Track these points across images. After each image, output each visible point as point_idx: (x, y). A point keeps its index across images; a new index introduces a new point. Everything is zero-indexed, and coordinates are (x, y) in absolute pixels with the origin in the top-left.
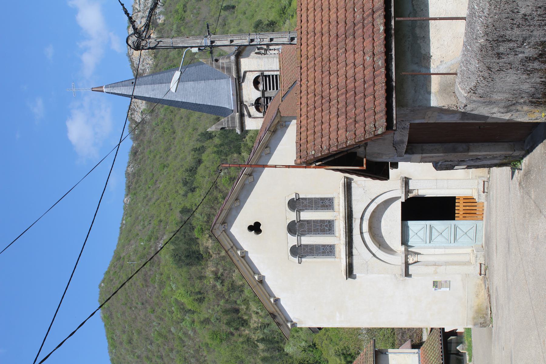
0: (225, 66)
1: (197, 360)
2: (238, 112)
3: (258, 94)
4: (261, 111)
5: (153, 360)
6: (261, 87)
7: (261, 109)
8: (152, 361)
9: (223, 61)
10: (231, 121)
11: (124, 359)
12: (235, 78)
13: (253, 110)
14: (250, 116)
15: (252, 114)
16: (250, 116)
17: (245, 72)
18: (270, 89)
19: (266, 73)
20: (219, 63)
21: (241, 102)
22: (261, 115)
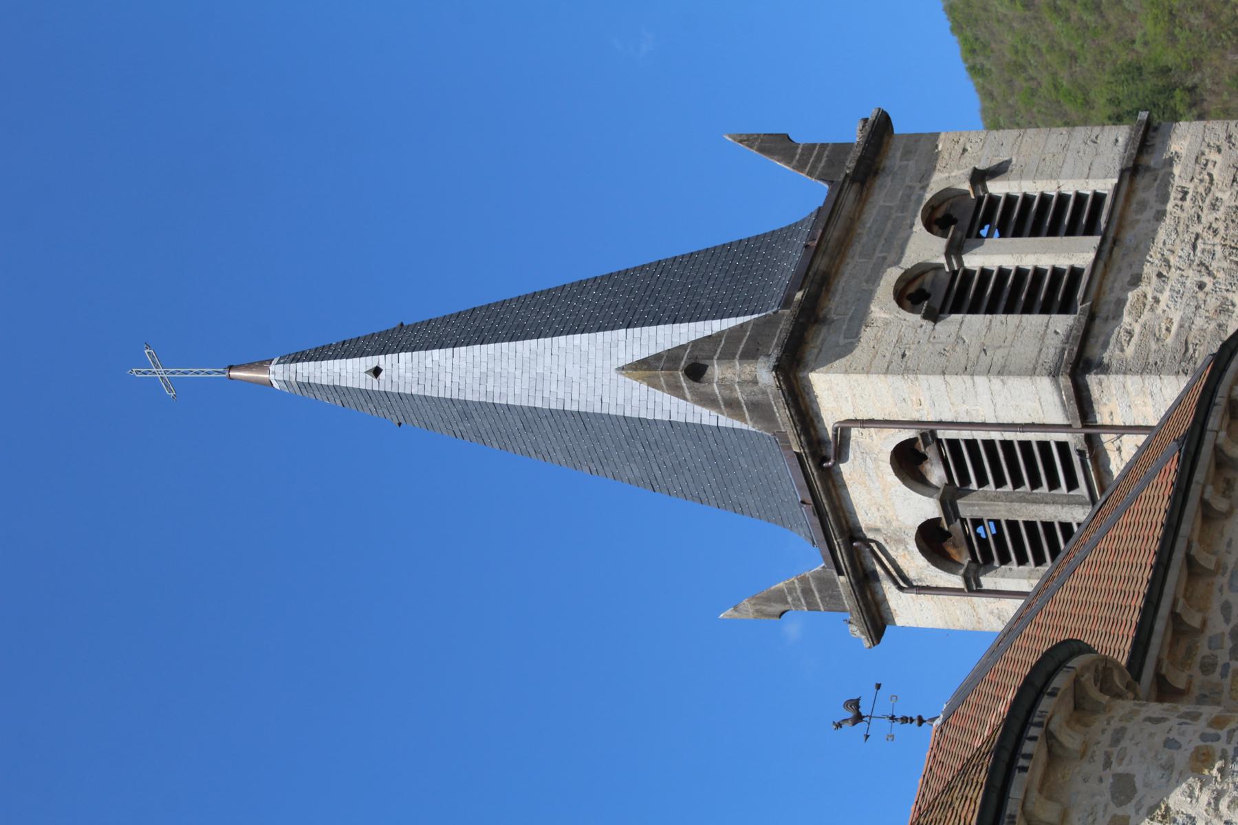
0: (739, 394)
1: (1211, 17)
2: (840, 573)
3: (929, 508)
4: (957, 558)
5: (1074, 17)
6: (936, 474)
7: (952, 551)
8: (1068, 19)
9: (729, 374)
10: (820, 591)
11: (985, 10)
12: (799, 455)
13: (915, 563)
14: (905, 583)
15: (912, 574)
16: (905, 583)
17: (843, 433)
18: (982, 481)
19: (943, 434)
20: (710, 383)
21: (852, 534)
22: (956, 581)
